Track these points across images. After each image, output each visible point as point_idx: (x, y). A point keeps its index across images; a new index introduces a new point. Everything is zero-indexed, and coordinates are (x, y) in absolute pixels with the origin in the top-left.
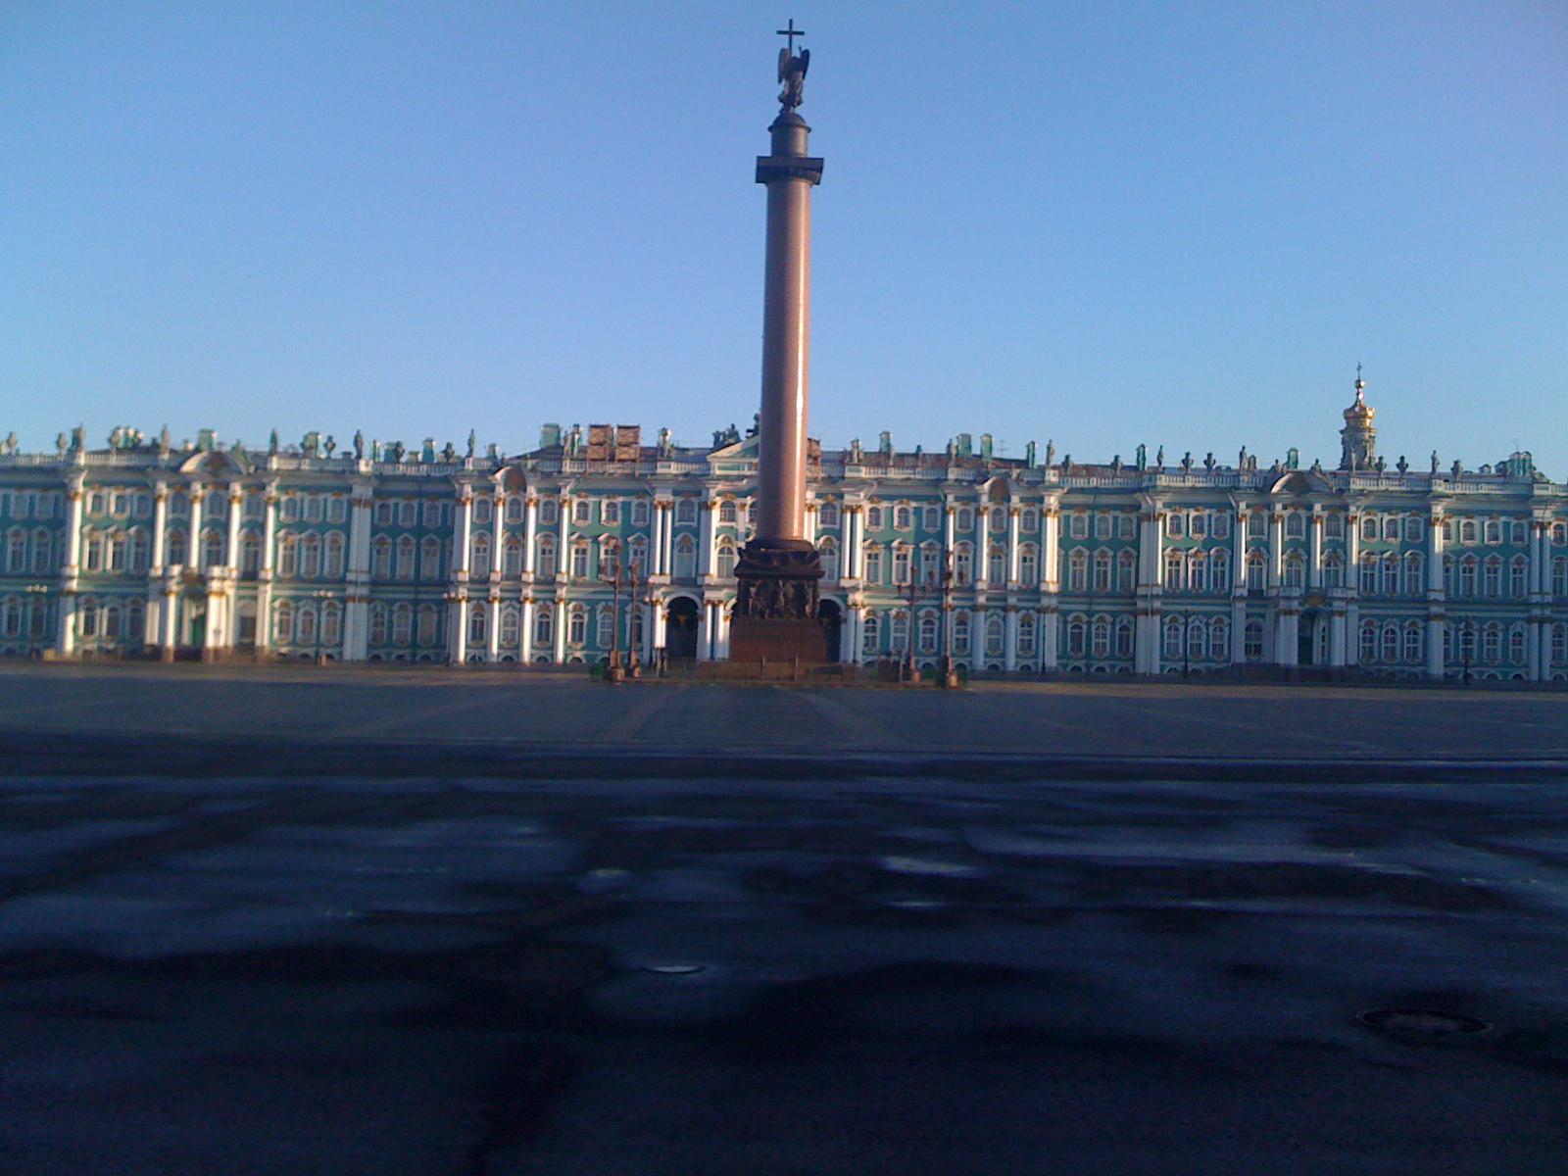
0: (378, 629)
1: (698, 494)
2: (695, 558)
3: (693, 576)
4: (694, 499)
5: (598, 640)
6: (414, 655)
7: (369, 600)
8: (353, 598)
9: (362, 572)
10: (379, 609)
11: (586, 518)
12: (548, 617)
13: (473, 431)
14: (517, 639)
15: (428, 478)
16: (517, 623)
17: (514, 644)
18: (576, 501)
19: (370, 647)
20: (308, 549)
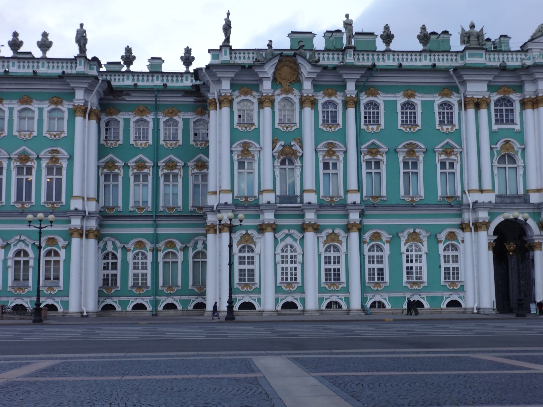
0: (110, 272)
1: (520, 88)
2: (520, 172)
3: (521, 192)
4: (515, 97)
5: (405, 279)
6: (155, 303)
7: (99, 237)
8: (80, 233)
9: (88, 199)
10: (110, 248)
11: (377, 122)
12: (337, 249)
13: (228, 14)
14: (299, 280)
15: (165, 89)
16: (299, 258)
17: (296, 286)
18: (364, 99)
19: (100, 294)
20: (20, 170)
